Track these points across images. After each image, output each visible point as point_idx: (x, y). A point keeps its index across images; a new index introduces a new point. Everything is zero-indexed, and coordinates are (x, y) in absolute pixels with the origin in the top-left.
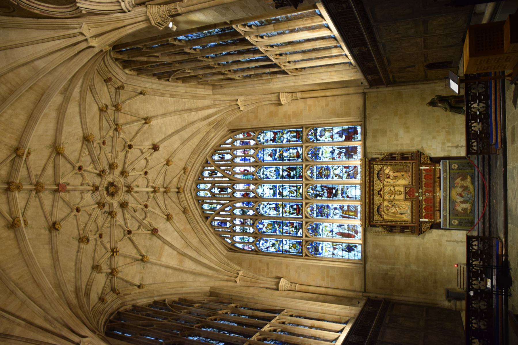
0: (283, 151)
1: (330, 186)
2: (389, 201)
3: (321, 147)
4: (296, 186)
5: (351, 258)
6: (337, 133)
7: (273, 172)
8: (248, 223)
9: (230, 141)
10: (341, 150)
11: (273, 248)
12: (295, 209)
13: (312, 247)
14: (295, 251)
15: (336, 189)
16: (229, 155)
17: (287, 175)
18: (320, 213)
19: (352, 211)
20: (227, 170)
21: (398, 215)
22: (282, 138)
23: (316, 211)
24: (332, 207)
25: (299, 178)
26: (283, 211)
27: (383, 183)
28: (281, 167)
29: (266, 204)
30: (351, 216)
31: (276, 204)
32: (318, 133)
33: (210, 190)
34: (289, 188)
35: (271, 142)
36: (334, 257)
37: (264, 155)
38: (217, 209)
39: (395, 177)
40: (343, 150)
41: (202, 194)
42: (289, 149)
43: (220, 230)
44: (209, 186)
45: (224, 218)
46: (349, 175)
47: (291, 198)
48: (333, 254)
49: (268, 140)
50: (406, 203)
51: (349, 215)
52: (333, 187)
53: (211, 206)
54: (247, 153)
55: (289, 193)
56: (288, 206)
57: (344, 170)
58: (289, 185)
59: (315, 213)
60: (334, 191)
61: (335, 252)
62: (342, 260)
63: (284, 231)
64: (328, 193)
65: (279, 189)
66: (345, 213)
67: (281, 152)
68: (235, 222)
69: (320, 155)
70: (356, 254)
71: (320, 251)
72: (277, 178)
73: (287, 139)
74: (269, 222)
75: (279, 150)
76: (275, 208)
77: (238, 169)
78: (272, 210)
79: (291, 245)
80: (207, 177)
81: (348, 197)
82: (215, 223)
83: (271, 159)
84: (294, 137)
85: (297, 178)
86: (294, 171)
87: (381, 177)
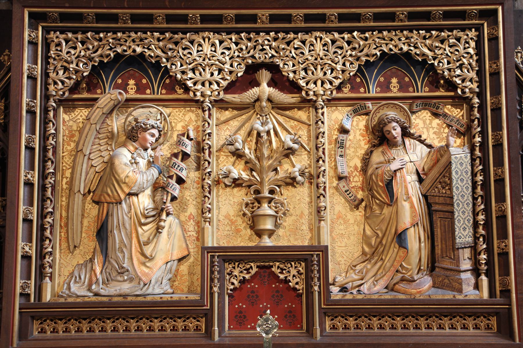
2: (200, 148)
21: (93, 210)
27: (331, 102)
39: (389, 185)
50: (184, 268)
87: (386, 86)
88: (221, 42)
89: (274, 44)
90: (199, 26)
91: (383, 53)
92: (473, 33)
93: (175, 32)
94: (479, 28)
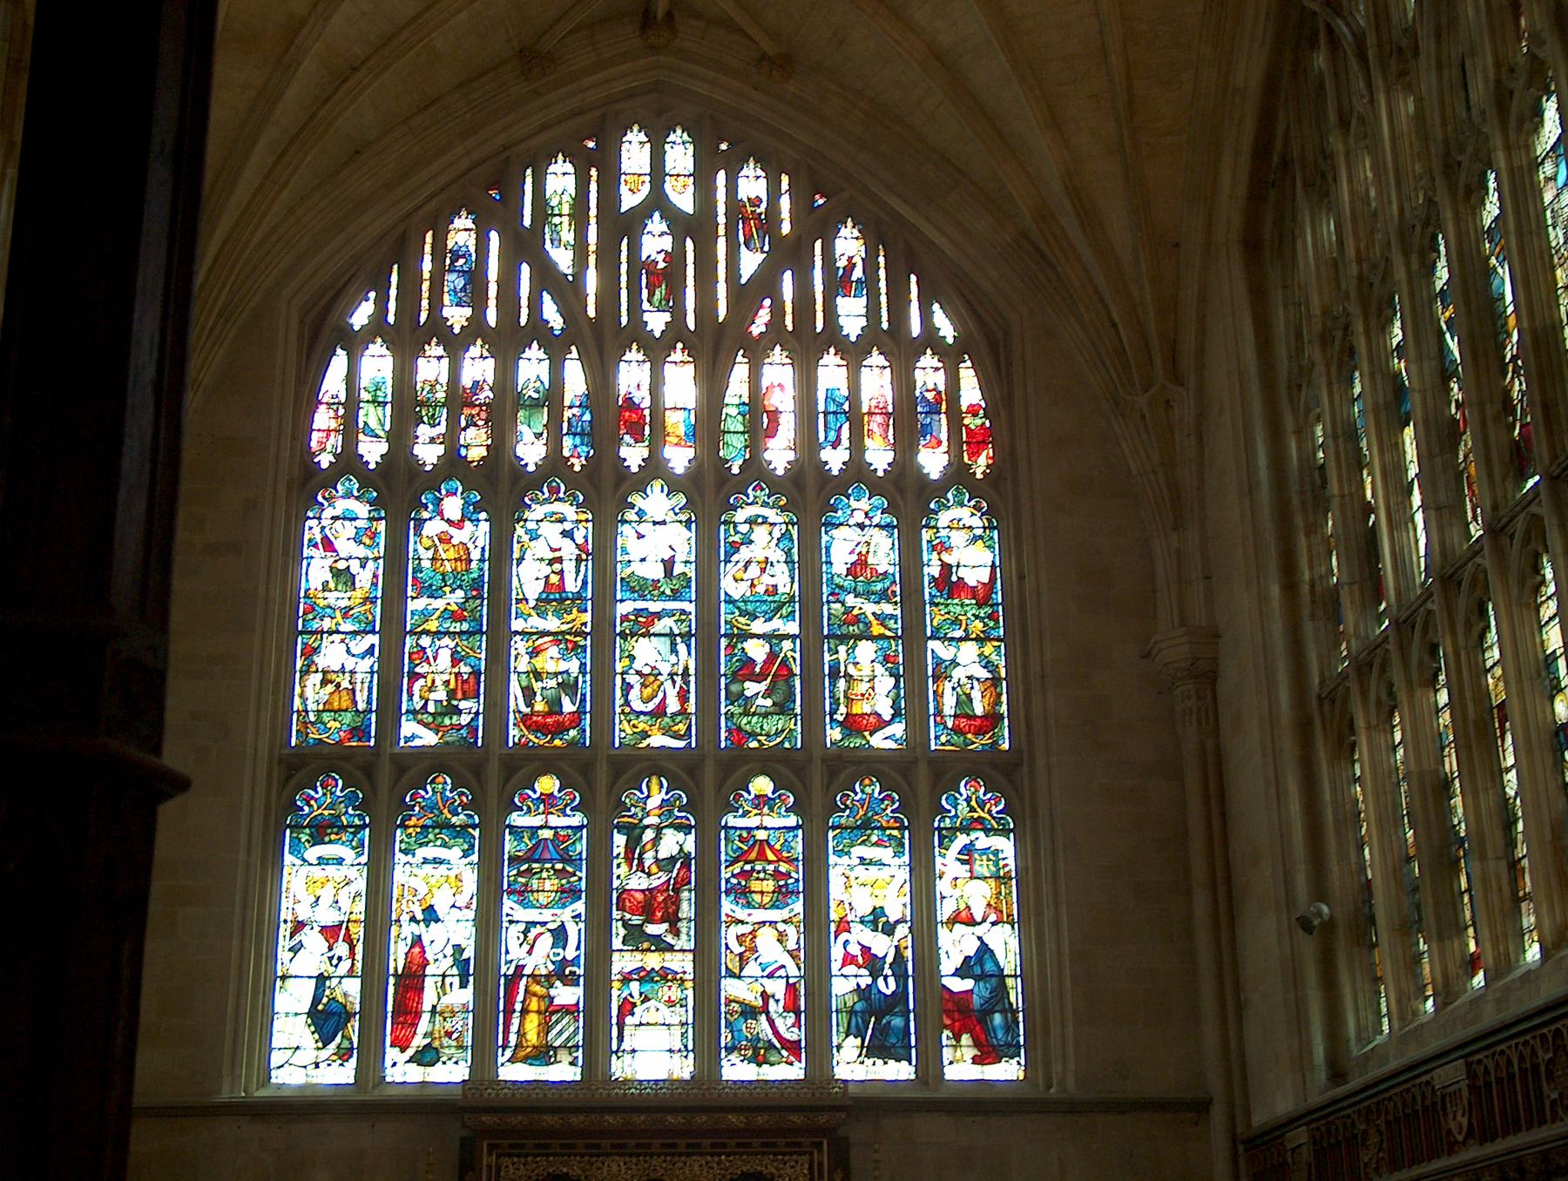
0: (881, 637)
1: (687, 910)
3: (906, 858)
4: (683, 712)
5: (277, 1025)
6: (984, 950)
7: (767, 580)
8: (472, 431)
9: (945, 328)
10: (888, 971)
11: (328, 577)
12: (555, 706)
13: (331, 806)
14: (311, 706)
15: (669, 939)
16: (863, 322)
17: (752, 662)
18: (536, 846)
19: (545, 1028)
20: (777, 311)
22: (959, 633)
23: (545, 826)
24: (566, 915)
25: (729, 730)
26: (543, 634)
28: (793, 628)
29: (579, 536)
30: (516, 1022)
31: (578, 596)
32: (982, 841)
33: (657, 201)
34: (672, 675)
35: (934, 570)
36: (285, 930)
37: (861, 526)
38: (548, 245)
40: (891, 980)
41: (635, 153)
42: (897, 677)
43: (427, 265)
44: (683, 199)
45: (493, 290)
46: (749, 1012)
47: (618, 679)
48: (299, 926)
49: (949, 549)
51: (525, 1012)
52: (683, 926)
53: (566, 209)
54: (874, 426)
55: (647, 670)
56: (573, 666)
57: (777, 988)
58: (692, 671)
59: (537, 821)
60: (652, 929)
61: (313, 941)
62: (266, 981)
63: (425, 641)
64: (650, 892)
65: (671, 614)
66: (537, 988)
67: (877, 629)
68: (475, 351)
69: (858, 851)
70: (299, 1058)
71: (312, 853)
72: (730, 601)
73: (954, 663)
74: (476, 555)
75: (892, 616)
76: (561, 587)
77: (779, 372)
78: (548, 570)
79: (345, 684)
80: (732, 188)
81: (627, 1007)
82: (462, 232)
83: (839, 567)
84: (964, 700)
85: (730, 716)
86: (769, 702)
88: (625, 1164)
89: (664, 1165)
90: (609, 1151)
91: (743, 1172)
92: (806, 1158)
93: (591, 1155)
94: (811, 1154)
